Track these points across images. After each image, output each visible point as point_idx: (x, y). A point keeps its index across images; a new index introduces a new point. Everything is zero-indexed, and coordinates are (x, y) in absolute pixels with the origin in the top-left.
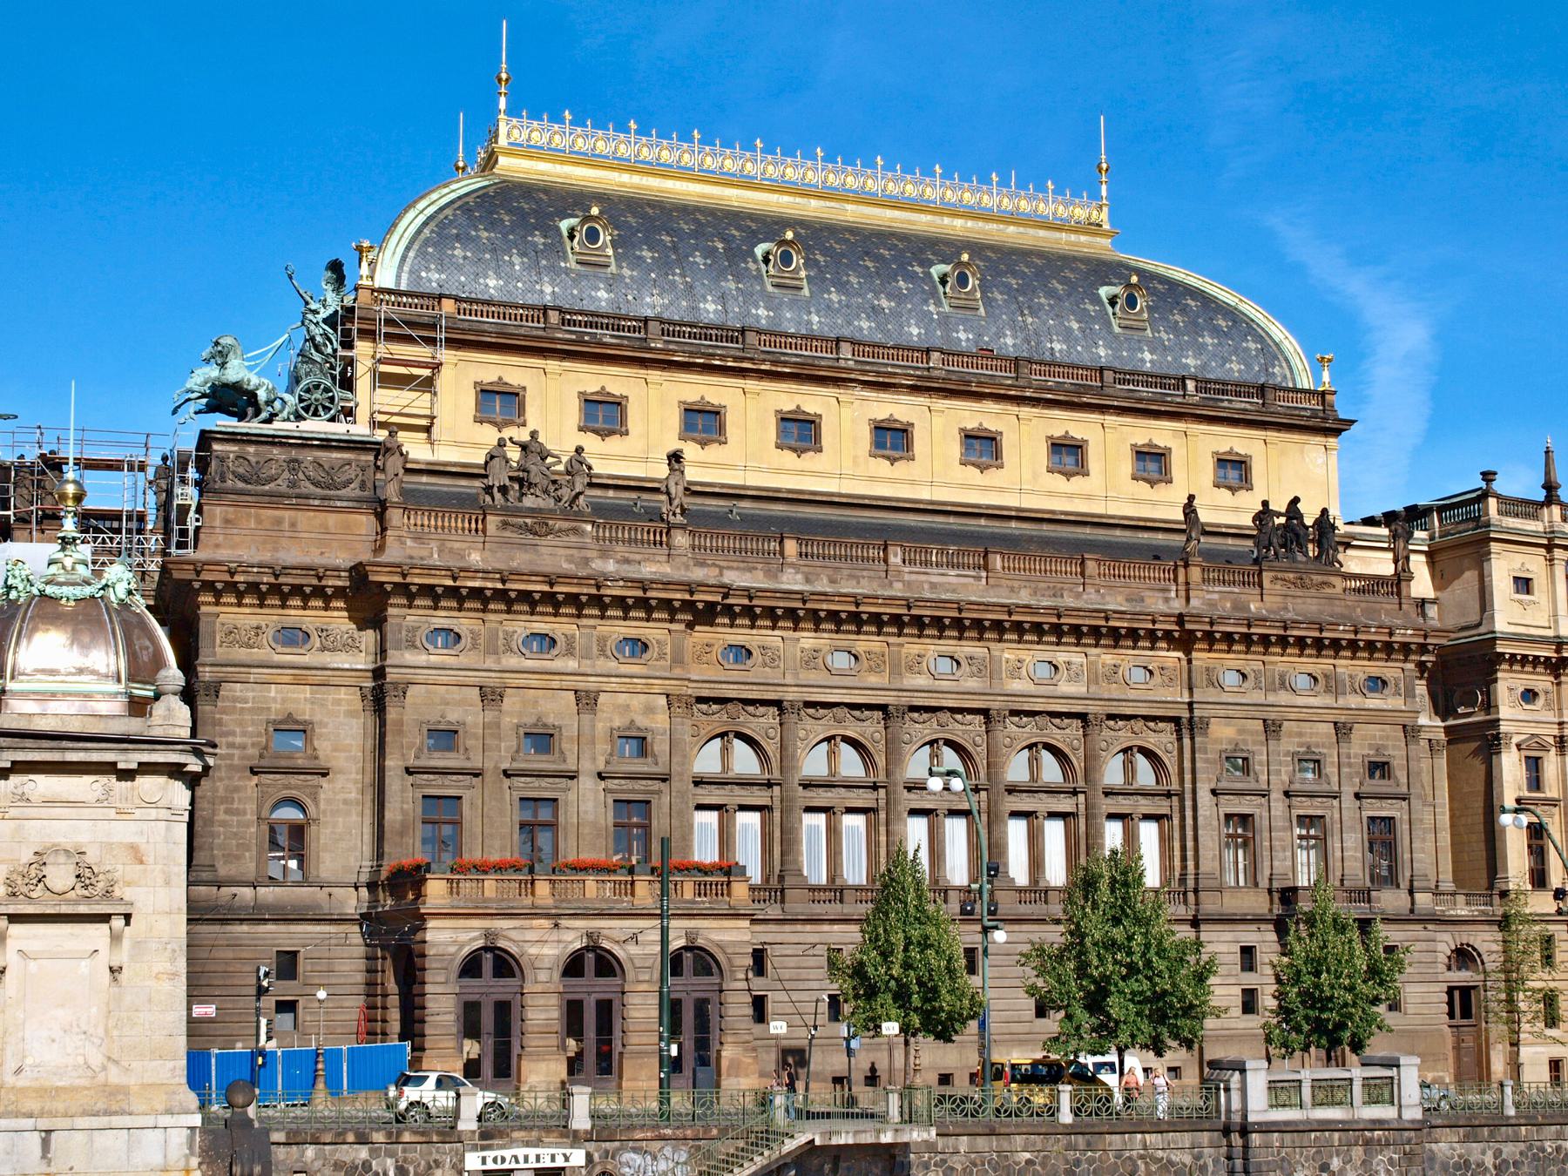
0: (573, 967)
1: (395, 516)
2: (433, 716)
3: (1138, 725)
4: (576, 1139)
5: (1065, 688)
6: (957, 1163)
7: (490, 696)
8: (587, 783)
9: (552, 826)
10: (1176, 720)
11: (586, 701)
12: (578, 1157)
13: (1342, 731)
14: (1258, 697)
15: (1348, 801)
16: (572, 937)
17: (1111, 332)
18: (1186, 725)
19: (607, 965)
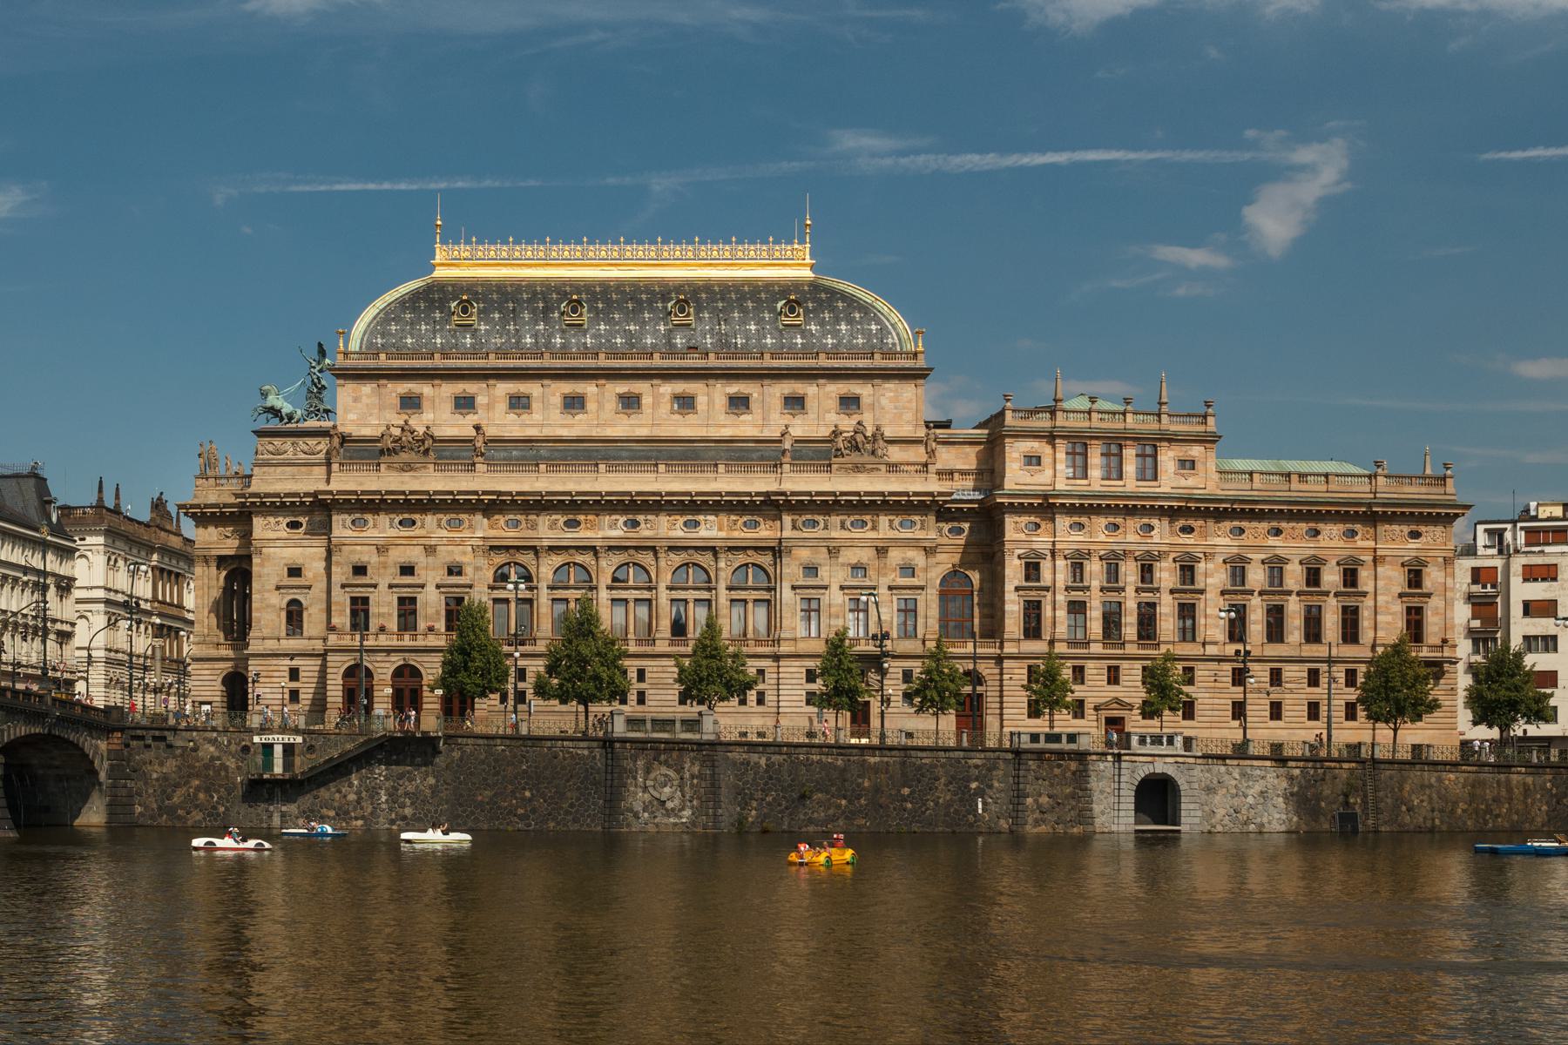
0: (398, 673)
1: (335, 467)
2: (355, 559)
3: (750, 552)
4: (296, 731)
5: (703, 532)
6: (468, 749)
7: (381, 549)
8: (430, 588)
9: (414, 612)
10: (772, 549)
11: (430, 550)
12: (299, 739)
13: (881, 551)
14: (824, 534)
15: (883, 591)
16: (397, 660)
17: (777, 328)
18: (777, 551)
19: (416, 673)
